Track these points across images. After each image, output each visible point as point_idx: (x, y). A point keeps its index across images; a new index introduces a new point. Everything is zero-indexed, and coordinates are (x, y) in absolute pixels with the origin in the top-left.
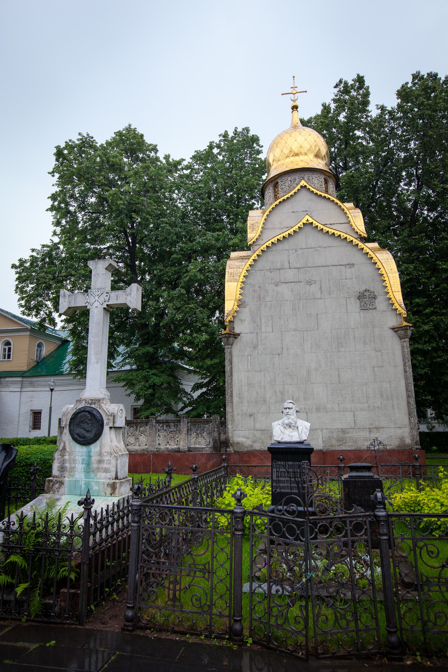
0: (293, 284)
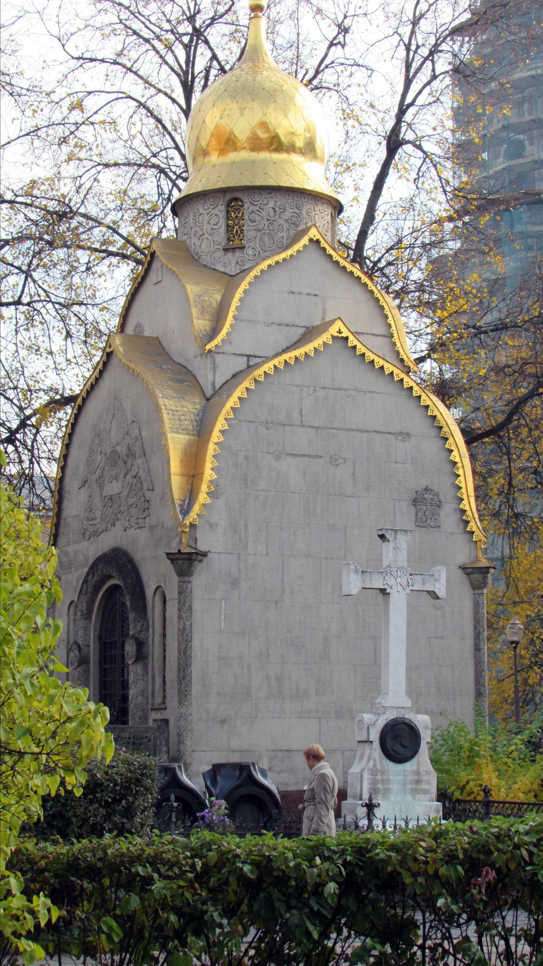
0: (306, 459)
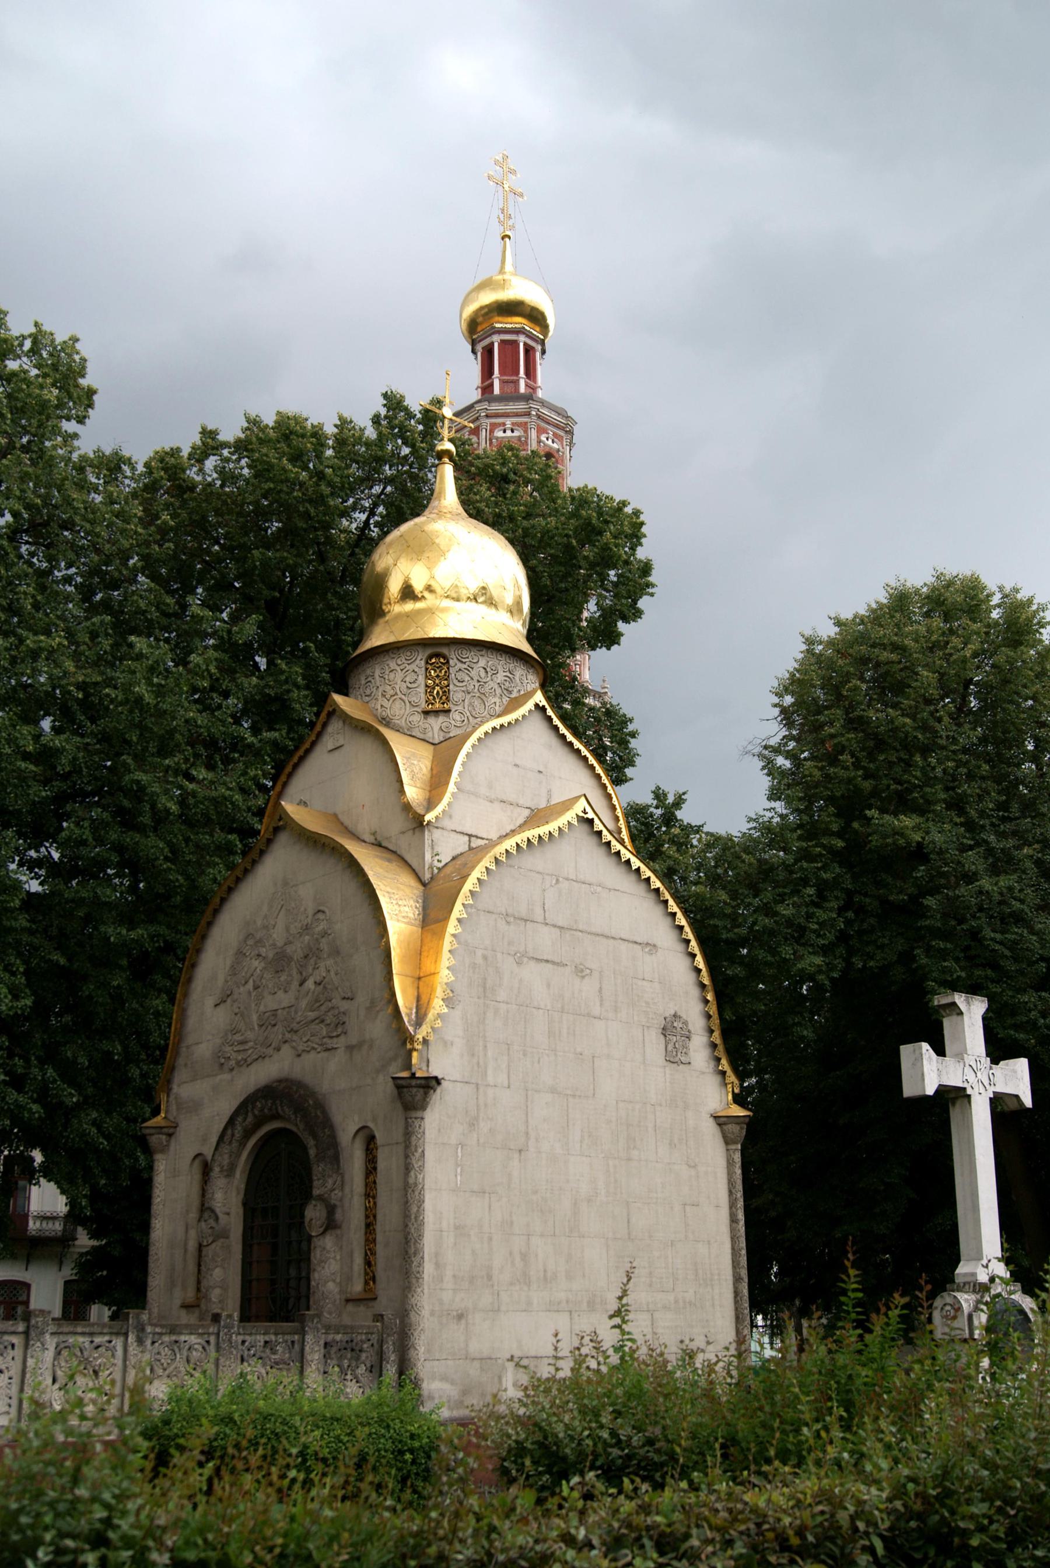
0: (549, 966)
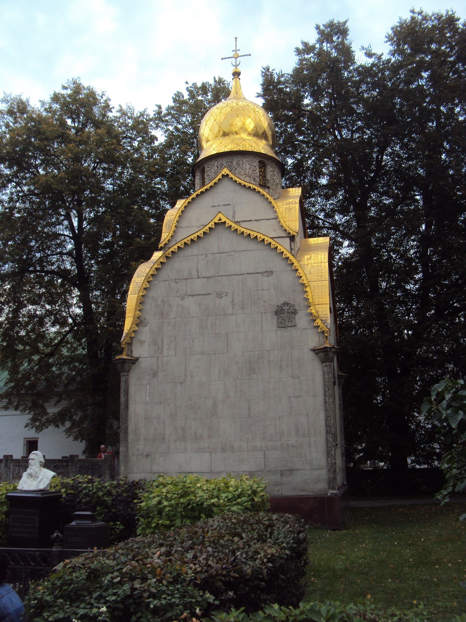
0: (201, 296)
